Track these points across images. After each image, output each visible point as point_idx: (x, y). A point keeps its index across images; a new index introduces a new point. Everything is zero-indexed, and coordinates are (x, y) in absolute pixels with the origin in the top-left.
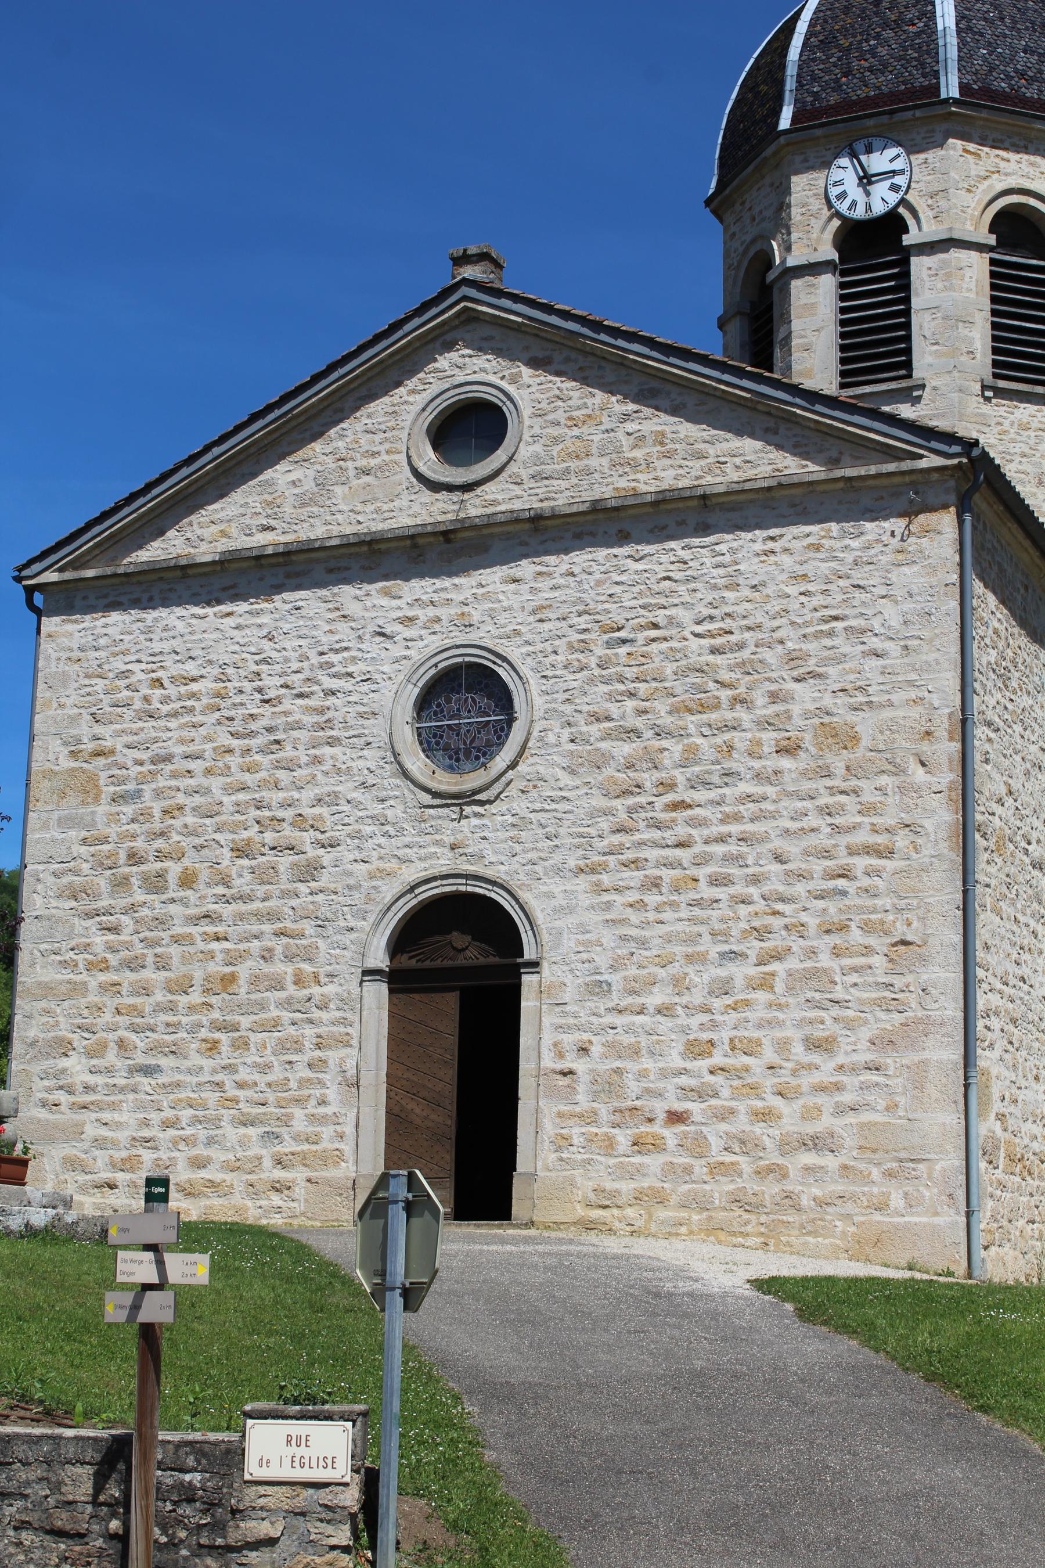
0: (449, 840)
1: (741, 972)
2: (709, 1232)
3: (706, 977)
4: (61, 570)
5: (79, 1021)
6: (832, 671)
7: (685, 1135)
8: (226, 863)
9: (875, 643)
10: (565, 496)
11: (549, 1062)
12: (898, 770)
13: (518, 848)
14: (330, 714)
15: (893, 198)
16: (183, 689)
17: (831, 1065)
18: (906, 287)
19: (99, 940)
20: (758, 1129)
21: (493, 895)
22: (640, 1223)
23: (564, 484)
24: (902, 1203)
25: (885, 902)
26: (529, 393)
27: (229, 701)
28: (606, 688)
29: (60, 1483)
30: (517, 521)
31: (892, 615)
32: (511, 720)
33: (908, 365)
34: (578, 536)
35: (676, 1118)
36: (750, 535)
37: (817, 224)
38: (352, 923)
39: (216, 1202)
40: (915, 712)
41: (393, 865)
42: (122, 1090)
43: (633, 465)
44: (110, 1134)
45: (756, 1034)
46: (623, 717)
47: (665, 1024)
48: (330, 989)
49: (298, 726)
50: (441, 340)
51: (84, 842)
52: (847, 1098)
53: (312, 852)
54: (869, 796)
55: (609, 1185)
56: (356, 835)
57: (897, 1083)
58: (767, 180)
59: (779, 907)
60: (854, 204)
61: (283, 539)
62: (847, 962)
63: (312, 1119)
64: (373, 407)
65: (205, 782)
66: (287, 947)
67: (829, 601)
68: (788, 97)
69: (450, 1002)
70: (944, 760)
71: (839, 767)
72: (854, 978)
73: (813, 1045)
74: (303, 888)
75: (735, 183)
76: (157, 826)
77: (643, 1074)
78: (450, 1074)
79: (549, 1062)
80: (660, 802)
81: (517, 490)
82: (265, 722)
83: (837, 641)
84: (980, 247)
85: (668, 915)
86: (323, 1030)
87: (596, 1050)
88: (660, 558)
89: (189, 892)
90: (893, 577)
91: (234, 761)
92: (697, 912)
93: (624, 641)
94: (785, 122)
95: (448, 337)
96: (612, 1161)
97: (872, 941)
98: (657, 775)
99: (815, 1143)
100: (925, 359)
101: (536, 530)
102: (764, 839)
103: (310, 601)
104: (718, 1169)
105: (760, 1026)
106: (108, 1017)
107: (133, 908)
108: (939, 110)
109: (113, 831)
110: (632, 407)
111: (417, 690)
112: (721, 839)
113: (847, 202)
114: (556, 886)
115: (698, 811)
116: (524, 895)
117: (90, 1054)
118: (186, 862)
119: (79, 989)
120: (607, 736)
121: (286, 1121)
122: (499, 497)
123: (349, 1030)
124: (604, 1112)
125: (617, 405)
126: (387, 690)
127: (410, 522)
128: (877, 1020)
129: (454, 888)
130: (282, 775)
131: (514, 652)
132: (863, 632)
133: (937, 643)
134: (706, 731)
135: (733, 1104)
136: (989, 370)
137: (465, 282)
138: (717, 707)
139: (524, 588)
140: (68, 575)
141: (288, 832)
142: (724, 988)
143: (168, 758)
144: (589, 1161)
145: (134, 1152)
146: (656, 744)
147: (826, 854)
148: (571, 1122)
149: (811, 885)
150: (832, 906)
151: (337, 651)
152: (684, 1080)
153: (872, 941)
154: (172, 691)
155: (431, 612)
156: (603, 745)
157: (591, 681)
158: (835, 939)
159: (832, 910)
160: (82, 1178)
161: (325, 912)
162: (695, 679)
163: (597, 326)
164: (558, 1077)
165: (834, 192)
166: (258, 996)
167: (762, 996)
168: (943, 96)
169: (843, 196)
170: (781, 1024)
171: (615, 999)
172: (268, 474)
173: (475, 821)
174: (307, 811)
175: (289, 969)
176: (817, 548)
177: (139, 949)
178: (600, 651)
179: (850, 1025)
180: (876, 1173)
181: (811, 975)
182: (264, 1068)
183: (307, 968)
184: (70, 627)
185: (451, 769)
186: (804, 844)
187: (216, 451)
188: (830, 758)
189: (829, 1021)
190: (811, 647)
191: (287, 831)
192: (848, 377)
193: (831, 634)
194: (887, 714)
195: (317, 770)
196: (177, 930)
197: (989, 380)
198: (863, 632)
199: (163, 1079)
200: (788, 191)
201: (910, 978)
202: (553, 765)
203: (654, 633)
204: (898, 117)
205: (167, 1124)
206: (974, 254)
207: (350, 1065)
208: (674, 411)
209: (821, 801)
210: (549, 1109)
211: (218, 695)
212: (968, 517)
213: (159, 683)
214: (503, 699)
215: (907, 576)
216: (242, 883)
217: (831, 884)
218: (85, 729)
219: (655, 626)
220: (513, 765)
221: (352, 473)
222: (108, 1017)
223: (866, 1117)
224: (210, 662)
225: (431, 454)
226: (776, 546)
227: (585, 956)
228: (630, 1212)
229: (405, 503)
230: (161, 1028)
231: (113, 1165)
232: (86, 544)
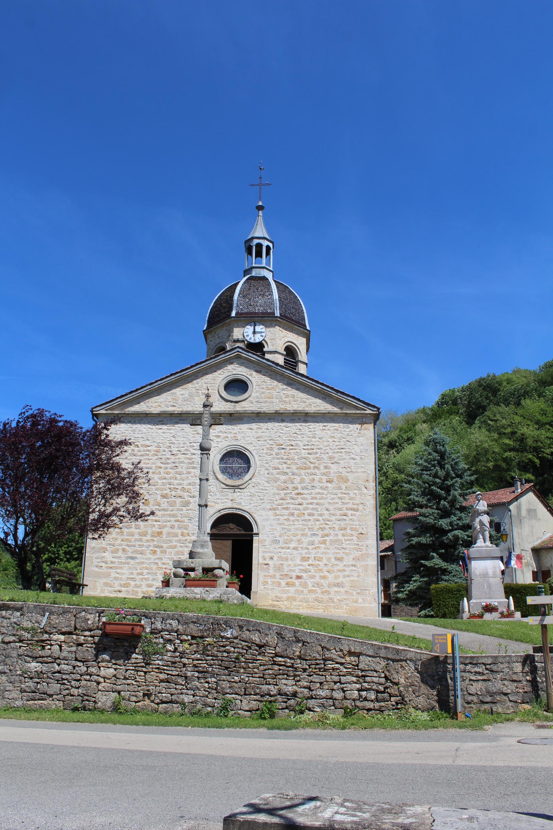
0: (230, 498)
1: (317, 539)
3: (307, 540)
4: (106, 410)
5: (110, 542)
6: (341, 462)
7: (301, 582)
8: (159, 499)
10: (266, 408)
12: (360, 489)
13: (252, 502)
14: (193, 460)
15: (261, 339)
16: (145, 449)
17: (342, 565)
20: (322, 581)
21: (244, 514)
23: (265, 405)
24: (362, 601)
26: (255, 379)
27: (161, 454)
28: (278, 461)
29: (512, 668)
30: (253, 413)
31: (357, 449)
32: (249, 467)
35: (298, 577)
36: (318, 424)
40: (364, 475)
42: (124, 563)
44: (120, 576)
45: (321, 556)
46: (283, 469)
47: (295, 552)
50: (230, 361)
52: (347, 573)
53: (187, 499)
54: (352, 495)
55: (279, 595)
58: (225, 328)
59: (328, 522)
60: (250, 338)
61: (178, 409)
62: (346, 538)
64: (207, 376)
66: (179, 525)
67: (340, 444)
69: (229, 543)
70: (372, 487)
71: (343, 487)
72: (348, 542)
73: (337, 559)
75: (214, 327)
77: (289, 565)
79: (261, 561)
80: (294, 492)
81: (251, 405)
82: (172, 460)
83: (342, 455)
85: (296, 523)
87: (275, 558)
89: (147, 507)
90: (357, 439)
91: (162, 471)
92: (304, 522)
93: (283, 449)
94: (233, 314)
95: (231, 361)
96: (280, 589)
97: (353, 533)
98: (293, 485)
99: (338, 585)
101: (257, 416)
102: (323, 504)
104: (311, 591)
105: (322, 554)
106: (119, 542)
108: (275, 319)
110: (285, 387)
111: (221, 456)
112: (311, 504)
113: (249, 338)
114: (263, 513)
115: (304, 496)
116: (254, 515)
117: (113, 552)
120: (278, 474)
122: (246, 406)
124: (278, 575)
125: (281, 386)
127: (219, 409)
128: (354, 553)
130: (177, 475)
132: (350, 453)
133: (369, 458)
134: (306, 474)
135: (315, 574)
137: (238, 347)
138: (310, 468)
140: (109, 412)
141: (179, 492)
142: (312, 543)
144: (273, 589)
145: (128, 582)
146: (293, 477)
147: (340, 509)
148: (268, 578)
149: (336, 517)
150: (342, 523)
151: (195, 443)
152: (301, 567)
153: (353, 533)
154: (141, 448)
155: (225, 435)
156: (277, 476)
157: (273, 458)
158: (343, 532)
159: (342, 524)
160: (110, 589)
162: (304, 460)
165: (245, 335)
166: (169, 538)
168: (276, 315)
169: (248, 336)
170: (328, 553)
171: (281, 545)
172: (174, 391)
173: (238, 494)
174: (185, 487)
175: (180, 531)
176: (337, 430)
178: (276, 450)
180: (354, 593)
183: (185, 531)
186: (334, 506)
187: (159, 382)
188: (341, 484)
189: (341, 553)
190: (336, 455)
193: (341, 452)
194: (356, 474)
198: (350, 453)
200: (232, 332)
201: (363, 543)
202: (262, 480)
203: (292, 447)
204: (264, 318)
205: (139, 574)
208: (297, 389)
210: (262, 574)
211: (157, 451)
214: (247, 460)
216: (165, 506)
219: (292, 445)
220: (250, 479)
221: (200, 394)
222: (119, 542)
223: (352, 578)
224: (154, 442)
226: (326, 428)
227: (272, 533)
228: (285, 602)
229: (217, 404)
230: (137, 546)
231: (121, 585)
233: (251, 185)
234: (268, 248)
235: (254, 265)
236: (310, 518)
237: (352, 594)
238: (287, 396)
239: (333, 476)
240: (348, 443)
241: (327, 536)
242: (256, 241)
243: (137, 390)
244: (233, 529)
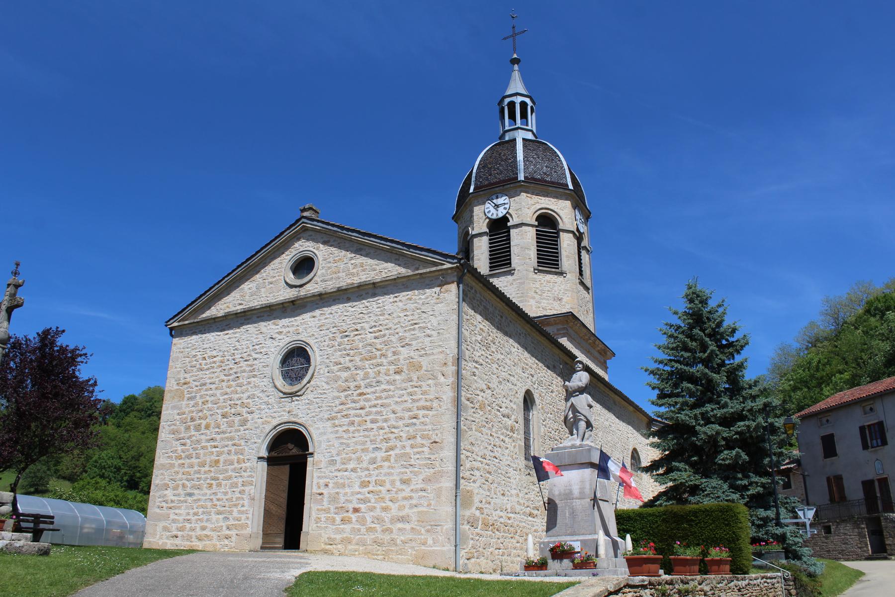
1: (380, 455)
2: (365, 554)
6: (414, 343)
9: (428, 332)
11: (315, 490)
15: (505, 212)
17: (409, 489)
18: (509, 239)
19: (180, 448)
20: (383, 514)
22: (342, 551)
25: (429, 427)
26: (322, 253)
30: (314, 296)
33: (510, 263)
34: (334, 300)
35: (356, 510)
37: (481, 221)
39: (208, 542)
40: (441, 356)
41: (269, 419)
42: (182, 502)
43: (353, 274)
47: (354, 475)
48: (248, 464)
49: (244, 371)
50: (296, 237)
51: (178, 414)
52: (414, 502)
55: (333, 536)
56: (259, 409)
57: (431, 496)
59: (393, 430)
62: (415, 450)
63: (240, 512)
65: (215, 392)
68: (473, 183)
69: (286, 469)
70: (450, 373)
71: (415, 378)
72: (418, 456)
73: (403, 482)
74: (242, 428)
76: (200, 408)
77: (346, 494)
82: (234, 370)
84: (532, 226)
85: (356, 435)
86: (245, 479)
87: (331, 485)
88: (359, 306)
91: (224, 384)
92: (366, 433)
94: (471, 191)
97: (424, 442)
98: (355, 383)
99: (402, 519)
100: (515, 261)
102: (389, 405)
103: (251, 328)
104: (370, 530)
105: (385, 475)
106: (180, 476)
107: (190, 437)
108: (518, 184)
109: (187, 410)
112: (375, 406)
114: (320, 425)
116: (310, 429)
118: (208, 420)
119: (172, 466)
120: (339, 370)
121: (231, 512)
125: (349, 255)
126: (272, 357)
130: (238, 388)
131: (311, 341)
136: (536, 264)
138: (376, 358)
139: (316, 319)
140: (180, 323)
141: (239, 409)
142: (373, 461)
143: (204, 384)
146: (355, 372)
147: (410, 410)
152: (359, 496)
153: (424, 442)
154: (208, 361)
155: (287, 329)
156: (338, 373)
157: (335, 351)
158: (410, 442)
159: (411, 431)
161: (248, 437)
162: (369, 348)
163: (342, 228)
165: (486, 211)
167: (386, 464)
169: (489, 212)
170: (392, 474)
171: (338, 466)
174: (245, 401)
175: (236, 458)
176: (410, 299)
177: (191, 451)
178: (339, 340)
179: (416, 474)
180: (423, 531)
181: (405, 455)
182: (226, 493)
183: (241, 457)
184: (181, 341)
185: (291, 384)
190: (407, 334)
191: (239, 409)
192: (492, 268)
193: (414, 329)
194: (432, 357)
195: (249, 386)
196: (203, 444)
197: (536, 267)
199: (195, 498)
201: (437, 455)
203: (356, 333)
205: (195, 514)
206: (530, 228)
207: (252, 491)
208: (366, 256)
209: (408, 391)
210: (315, 507)
212: (461, 285)
213: (204, 358)
214: (307, 359)
215: (440, 307)
217: (411, 421)
218: (182, 375)
219: (357, 330)
220: (309, 382)
223: (420, 509)
225: (292, 276)
228: (339, 546)
232: (186, 312)
233: (505, 39)
234: (523, 105)
235: (507, 128)
236: (374, 426)
237: (420, 533)
238: (355, 266)
239: (403, 364)
240: (424, 315)
241: (392, 449)
242: (507, 100)
243: (206, 292)
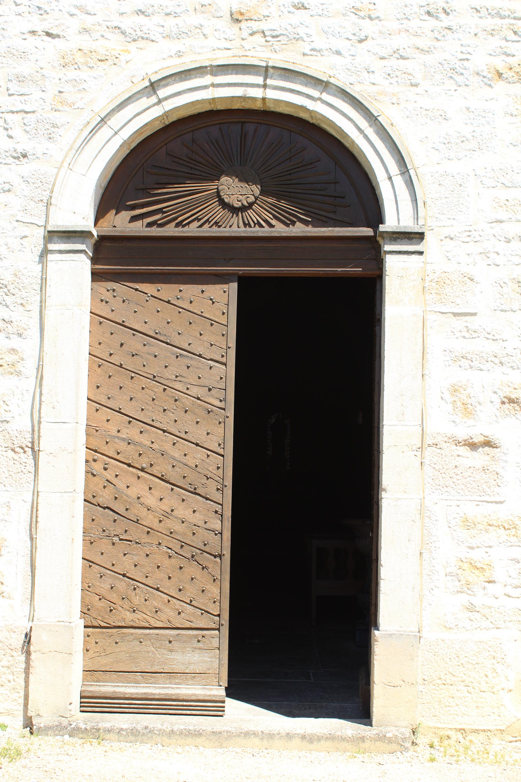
11: (442, 423)
13: (368, 28)
38: (24, 144)
69: (220, 302)
78: (221, 434)
116: (387, 114)
123: (15, 342)
129: (238, 92)
164: (464, 451)
244: (236, 207)
